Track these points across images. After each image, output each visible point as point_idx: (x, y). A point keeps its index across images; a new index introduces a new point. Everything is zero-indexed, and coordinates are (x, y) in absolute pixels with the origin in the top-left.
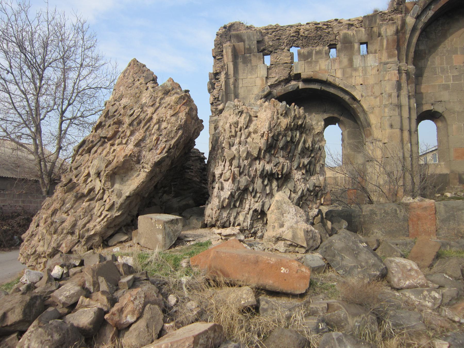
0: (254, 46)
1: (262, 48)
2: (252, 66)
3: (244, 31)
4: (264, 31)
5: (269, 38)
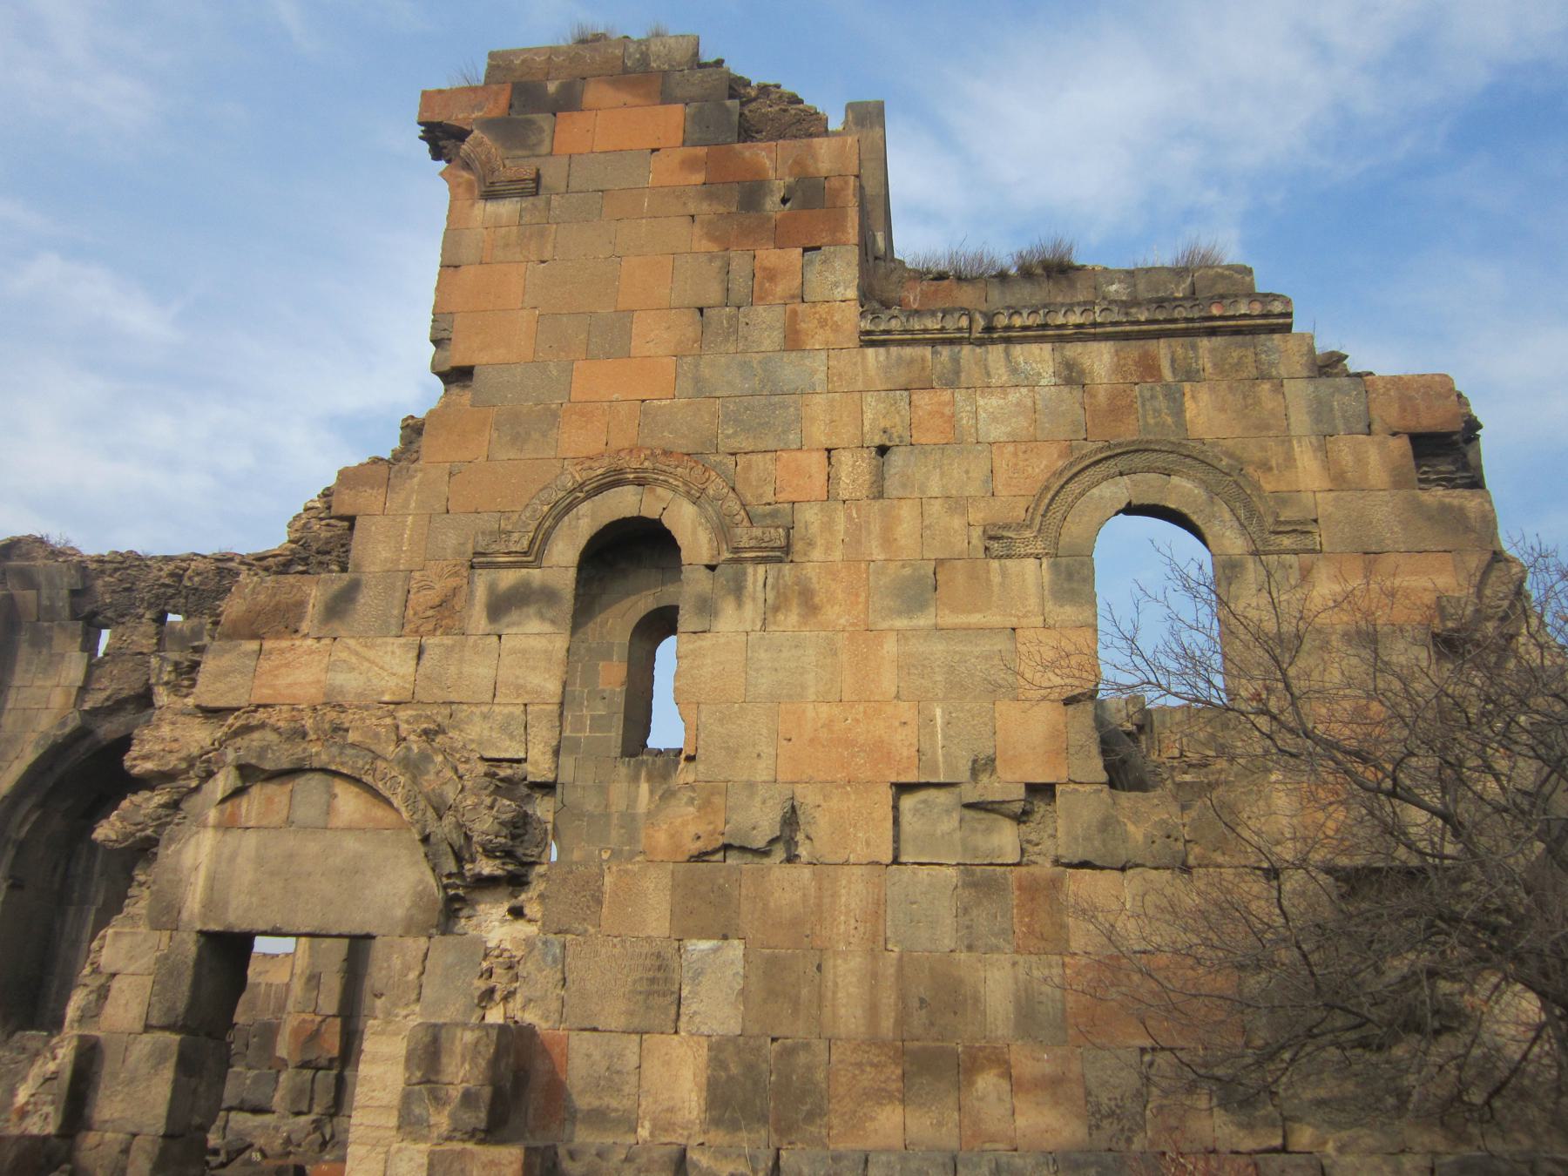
0: (63, 604)
1: (88, 609)
2: (52, 655)
3: (39, 563)
4: (94, 566)
5: (107, 584)
